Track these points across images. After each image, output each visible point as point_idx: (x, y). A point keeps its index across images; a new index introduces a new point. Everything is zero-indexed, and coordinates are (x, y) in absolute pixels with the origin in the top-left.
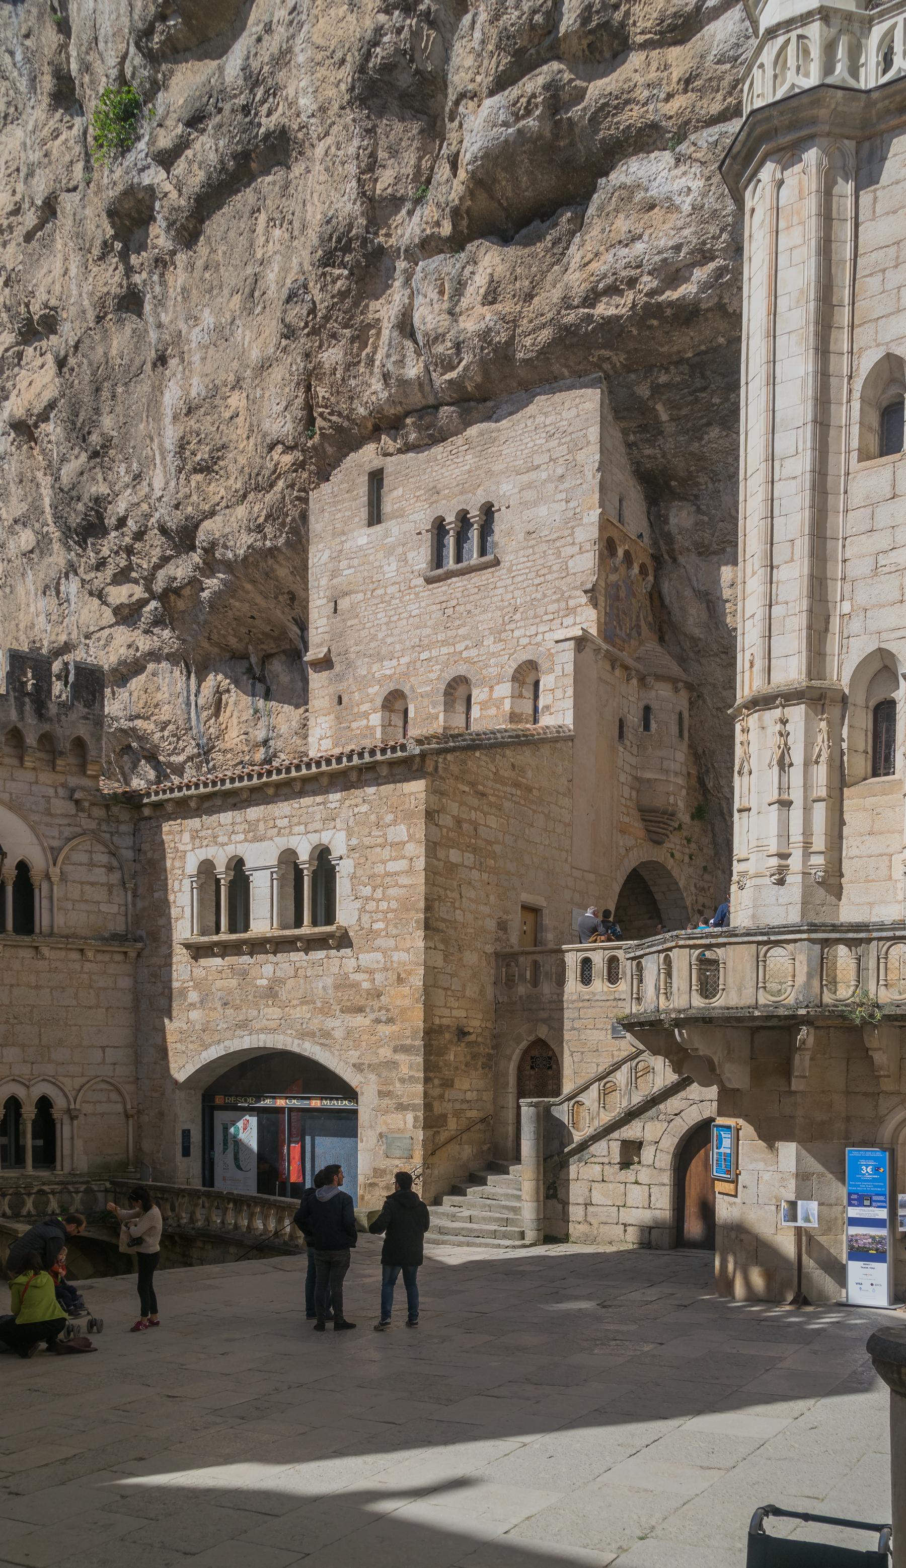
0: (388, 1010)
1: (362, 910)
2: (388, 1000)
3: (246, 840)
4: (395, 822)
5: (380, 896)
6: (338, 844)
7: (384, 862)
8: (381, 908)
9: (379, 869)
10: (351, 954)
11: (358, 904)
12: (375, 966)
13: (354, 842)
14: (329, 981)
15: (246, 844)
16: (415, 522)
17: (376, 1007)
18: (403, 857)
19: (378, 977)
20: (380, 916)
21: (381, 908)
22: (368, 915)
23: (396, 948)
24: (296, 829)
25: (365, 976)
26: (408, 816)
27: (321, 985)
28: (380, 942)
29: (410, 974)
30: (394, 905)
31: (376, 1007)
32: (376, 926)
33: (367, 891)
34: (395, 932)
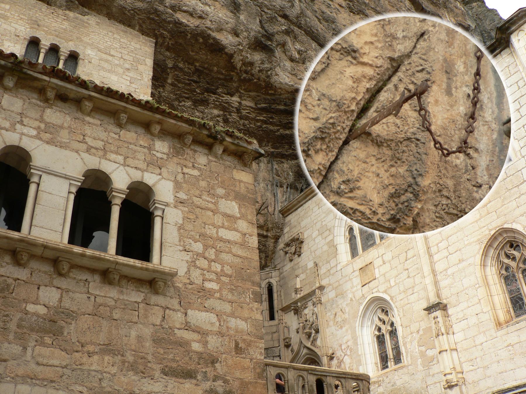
0: (226, 381)
1: (192, 264)
2: (225, 369)
3: (38, 137)
4: (226, 197)
5: (213, 257)
6: (164, 190)
7: (213, 225)
8: (213, 268)
9: (211, 231)
10: (177, 307)
11: (187, 257)
12: (209, 327)
13: (182, 196)
14: (147, 332)
15: (38, 142)
16: (16, 29)
17: (211, 374)
18: (236, 230)
19: (213, 342)
20: (213, 276)
21: (213, 268)
22: (198, 272)
23: (232, 315)
24: (113, 156)
25: (195, 336)
26: (239, 197)
27: (133, 333)
28: (210, 303)
29: (249, 345)
30: (228, 270)
31: (211, 374)
32: (209, 285)
33: (198, 247)
34: (230, 297)
